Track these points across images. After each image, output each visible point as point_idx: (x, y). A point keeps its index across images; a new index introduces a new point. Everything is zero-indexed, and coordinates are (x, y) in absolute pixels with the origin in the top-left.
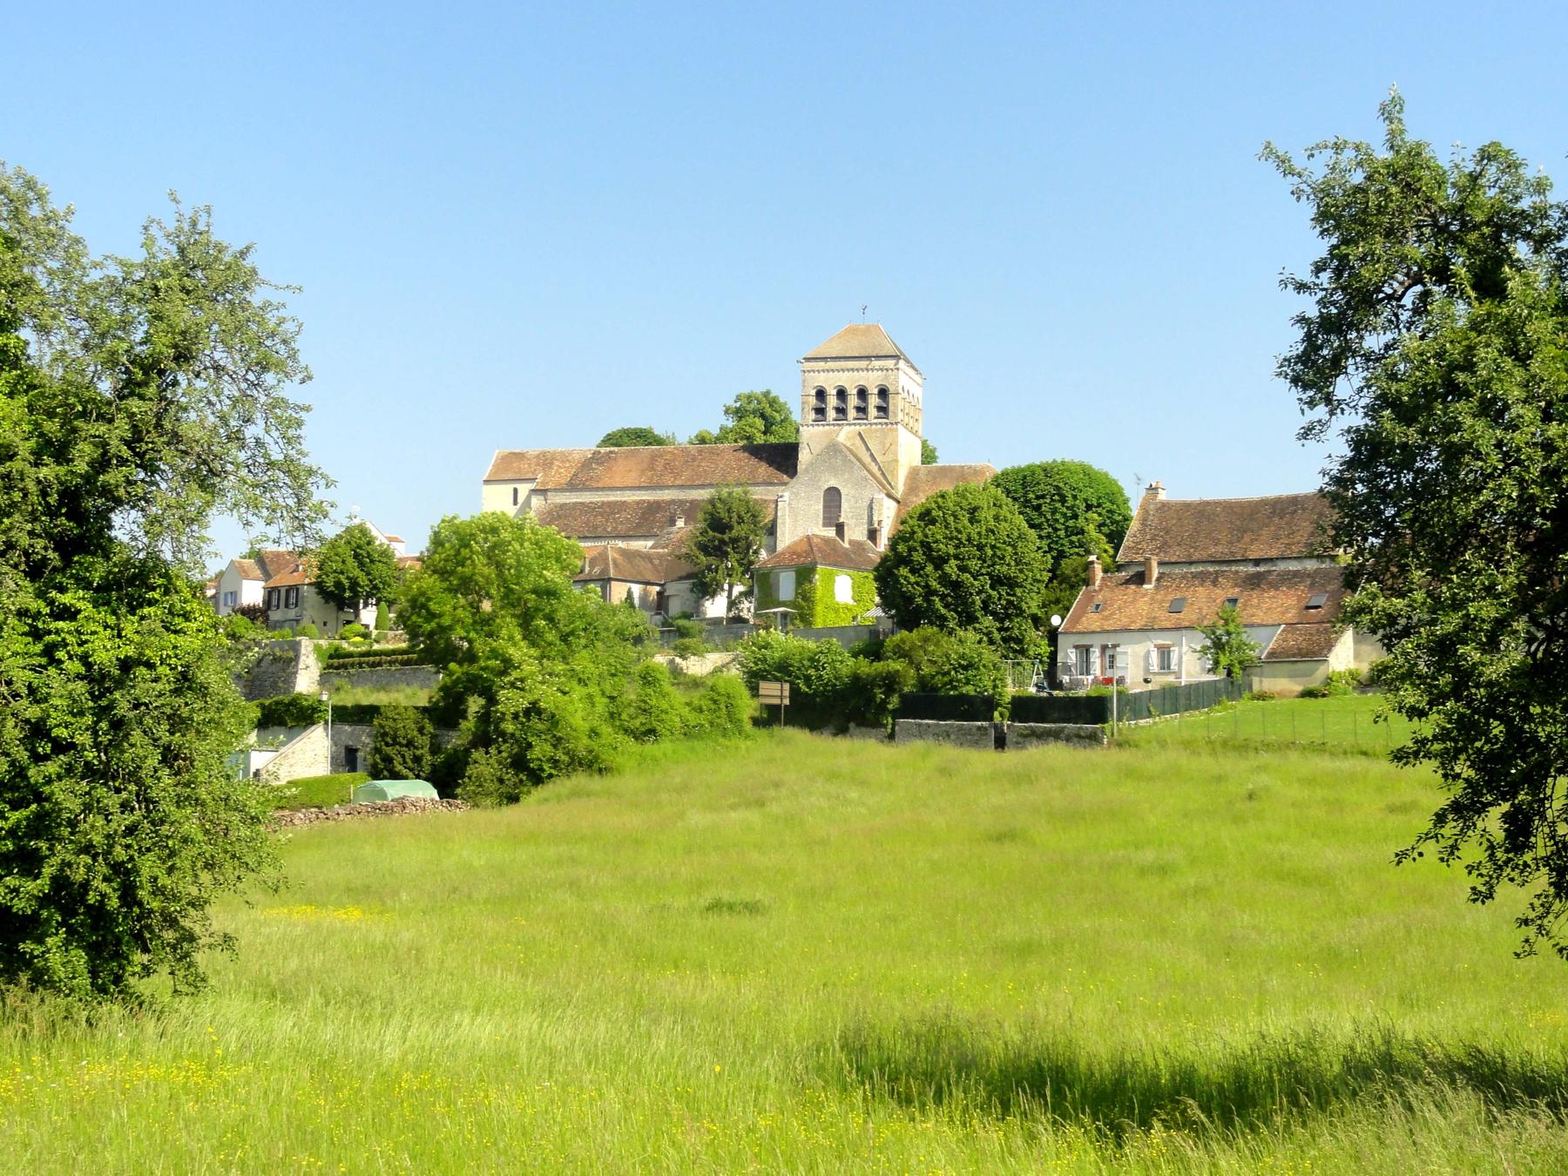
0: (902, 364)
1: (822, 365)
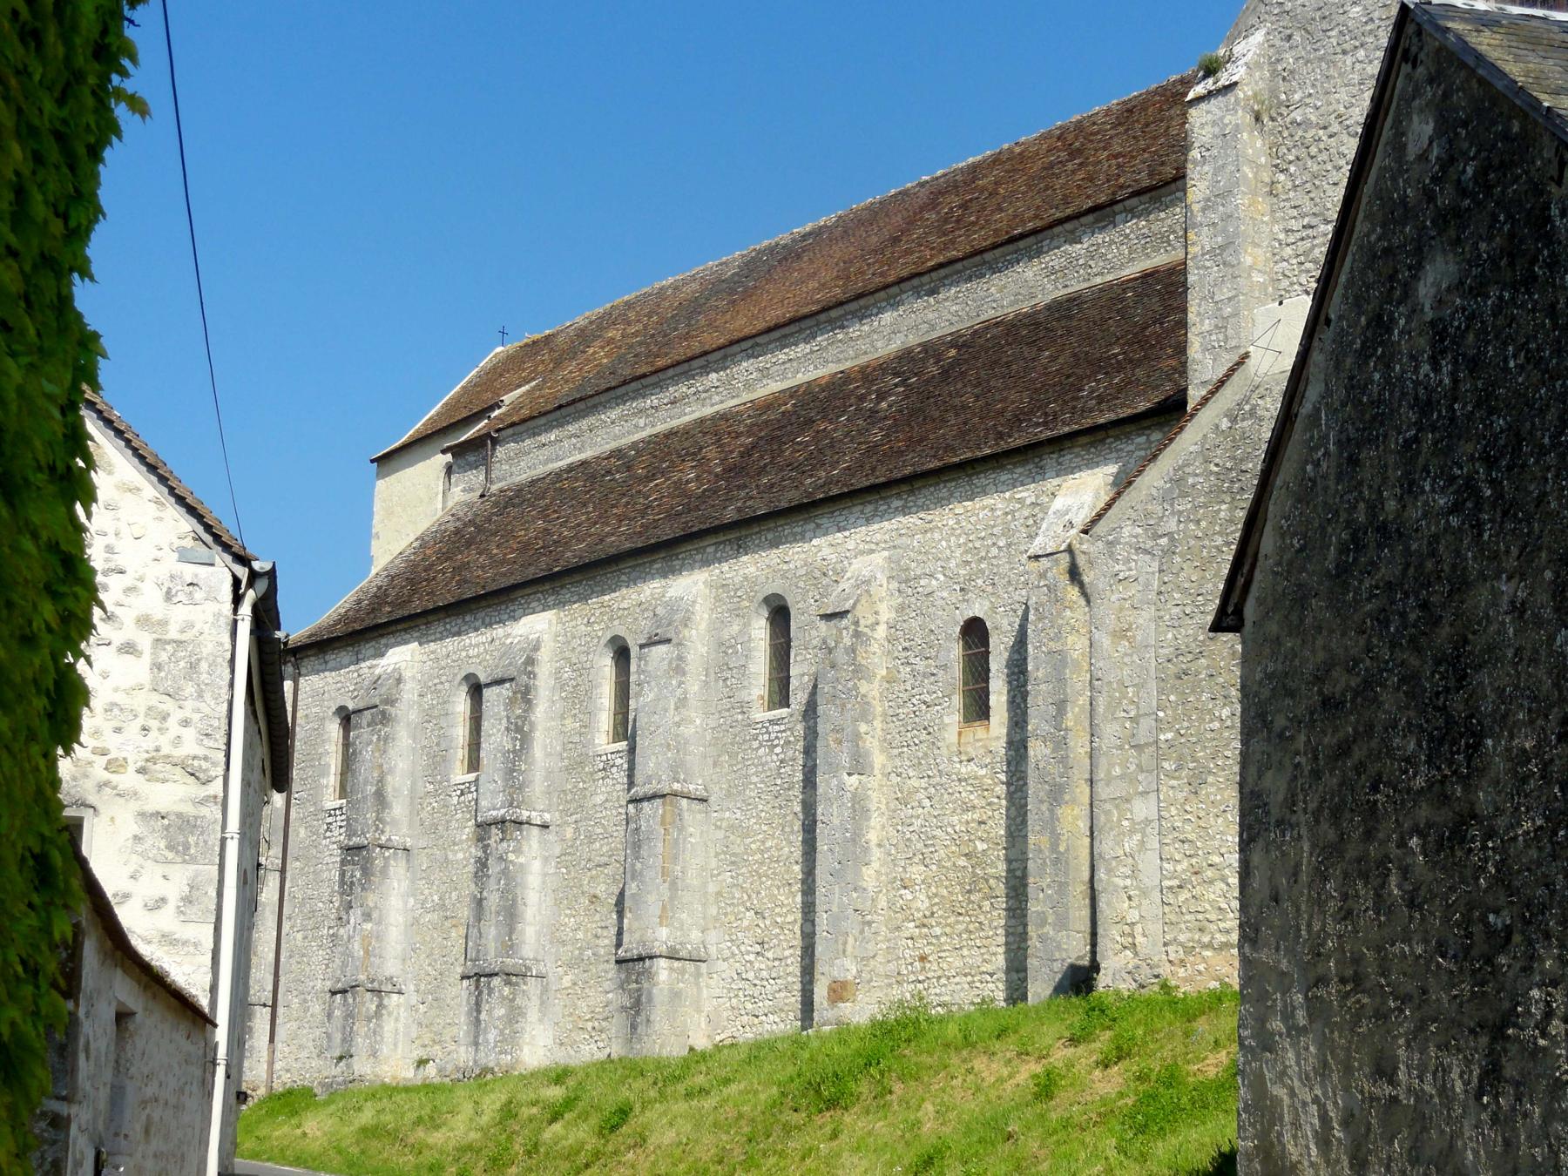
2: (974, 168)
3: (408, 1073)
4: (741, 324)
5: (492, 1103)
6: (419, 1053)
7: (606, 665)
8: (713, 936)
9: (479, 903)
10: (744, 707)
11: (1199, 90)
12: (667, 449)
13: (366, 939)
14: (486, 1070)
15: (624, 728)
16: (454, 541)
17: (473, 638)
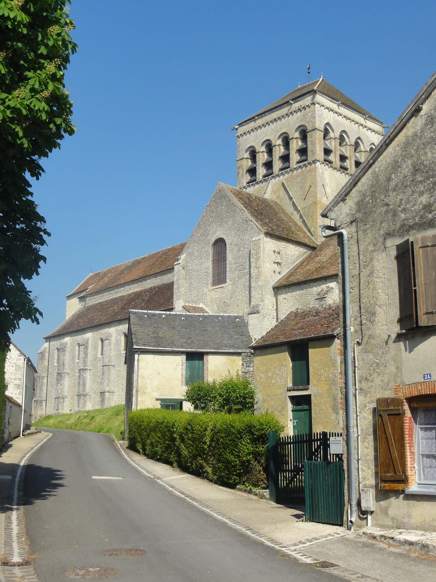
0: (319, 98)
1: (252, 125)
2: (169, 249)
3: (69, 412)
4: (128, 279)
5: (77, 416)
6: (70, 409)
7: (100, 342)
8: (115, 388)
9: (79, 383)
10: (120, 351)
11: (176, 263)
12: (114, 301)
13: (61, 389)
14: (80, 411)
15: (102, 354)
16: (79, 316)
17: (79, 337)
